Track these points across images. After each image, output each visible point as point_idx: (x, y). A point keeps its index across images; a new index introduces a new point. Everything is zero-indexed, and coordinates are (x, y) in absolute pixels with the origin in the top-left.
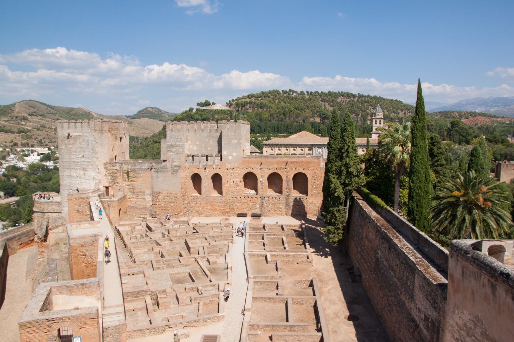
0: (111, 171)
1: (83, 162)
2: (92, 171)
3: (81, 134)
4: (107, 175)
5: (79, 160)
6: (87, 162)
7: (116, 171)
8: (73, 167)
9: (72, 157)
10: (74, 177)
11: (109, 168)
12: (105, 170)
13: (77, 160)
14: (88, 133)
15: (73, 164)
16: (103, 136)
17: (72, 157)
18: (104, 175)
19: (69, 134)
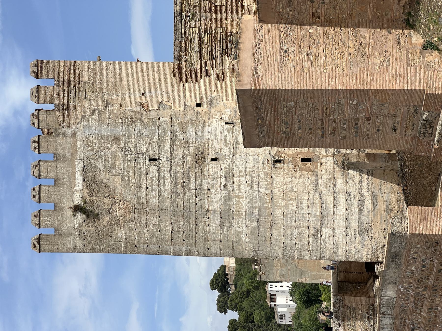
0: (207, 56)
1: (175, 161)
2: (207, 129)
3: (79, 165)
4: (219, 71)
5: (168, 175)
6: (172, 146)
7: (206, 38)
8: (192, 201)
9: (155, 201)
10: (227, 200)
11: (197, 63)
12: (203, 81)
13: (168, 182)
14: (74, 135)
15: (180, 201)
16: (85, 78)
17: (155, 201)
18: (219, 83)
19: (77, 209)
